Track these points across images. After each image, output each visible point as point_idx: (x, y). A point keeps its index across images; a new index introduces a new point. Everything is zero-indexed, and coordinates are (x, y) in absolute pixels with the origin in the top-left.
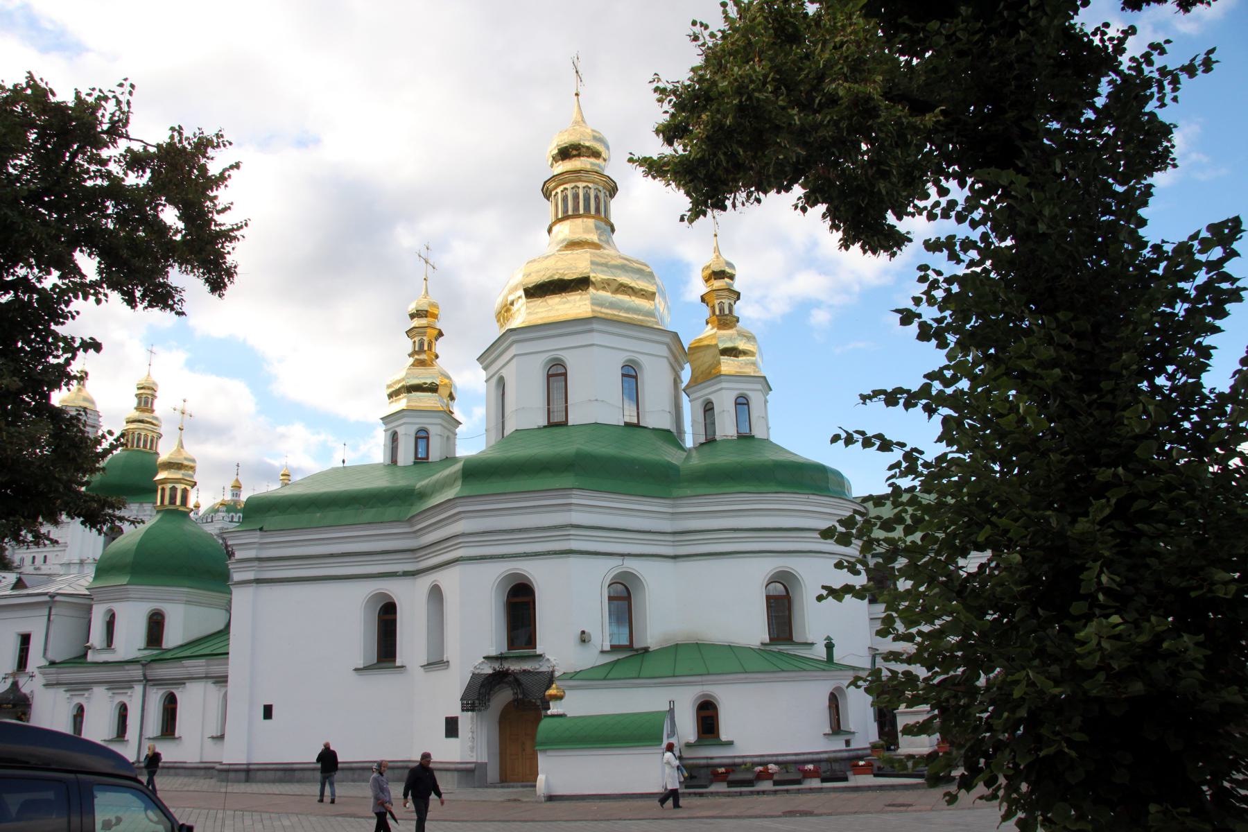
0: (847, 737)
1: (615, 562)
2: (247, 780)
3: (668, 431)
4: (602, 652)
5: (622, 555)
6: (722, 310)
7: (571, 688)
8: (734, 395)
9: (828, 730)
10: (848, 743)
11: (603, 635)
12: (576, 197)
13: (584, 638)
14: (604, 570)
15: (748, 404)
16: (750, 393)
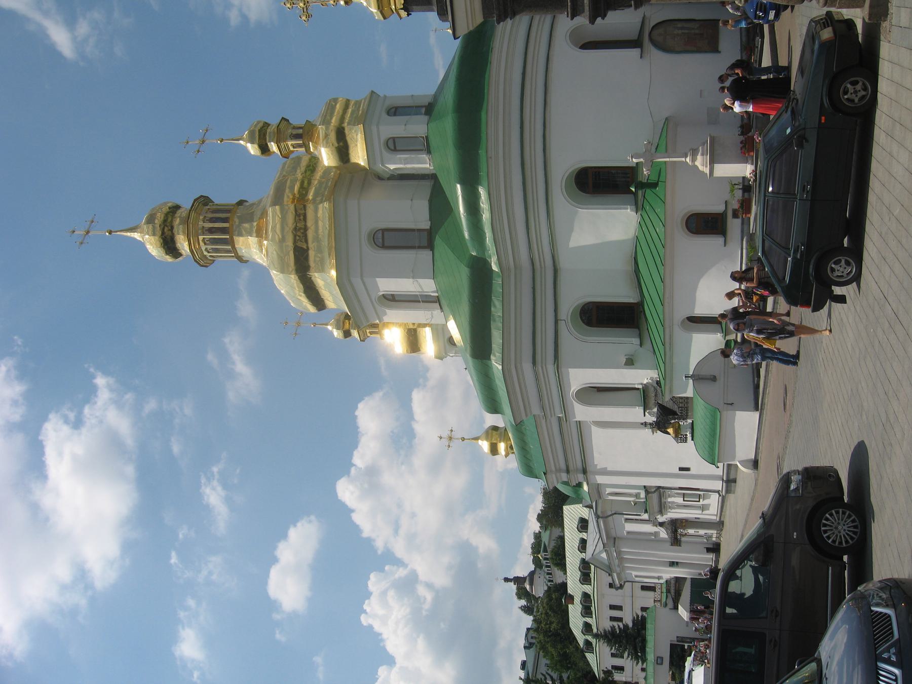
0: (730, 214)
1: (562, 325)
2: (735, 481)
3: (430, 201)
4: (641, 345)
5: (556, 321)
6: (300, 146)
7: (671, 391)
8: (387, 155)
9: (720, 240)
10: (735, 215)
11: (623, 342)
12: (211, 231)
13: (630, 362)
14: (573, 340)
15: (394, 139)
16: (384, 138)
